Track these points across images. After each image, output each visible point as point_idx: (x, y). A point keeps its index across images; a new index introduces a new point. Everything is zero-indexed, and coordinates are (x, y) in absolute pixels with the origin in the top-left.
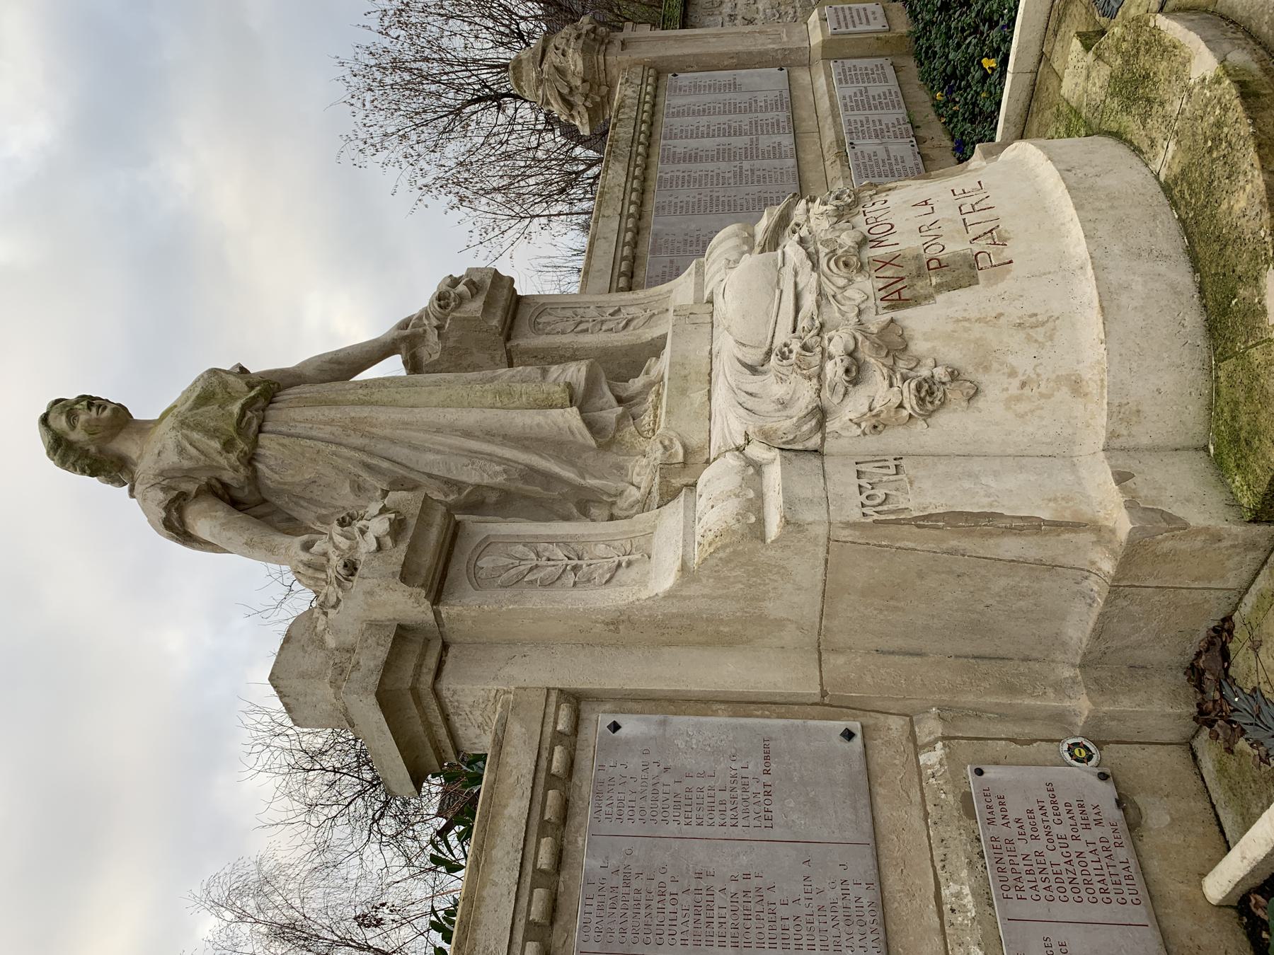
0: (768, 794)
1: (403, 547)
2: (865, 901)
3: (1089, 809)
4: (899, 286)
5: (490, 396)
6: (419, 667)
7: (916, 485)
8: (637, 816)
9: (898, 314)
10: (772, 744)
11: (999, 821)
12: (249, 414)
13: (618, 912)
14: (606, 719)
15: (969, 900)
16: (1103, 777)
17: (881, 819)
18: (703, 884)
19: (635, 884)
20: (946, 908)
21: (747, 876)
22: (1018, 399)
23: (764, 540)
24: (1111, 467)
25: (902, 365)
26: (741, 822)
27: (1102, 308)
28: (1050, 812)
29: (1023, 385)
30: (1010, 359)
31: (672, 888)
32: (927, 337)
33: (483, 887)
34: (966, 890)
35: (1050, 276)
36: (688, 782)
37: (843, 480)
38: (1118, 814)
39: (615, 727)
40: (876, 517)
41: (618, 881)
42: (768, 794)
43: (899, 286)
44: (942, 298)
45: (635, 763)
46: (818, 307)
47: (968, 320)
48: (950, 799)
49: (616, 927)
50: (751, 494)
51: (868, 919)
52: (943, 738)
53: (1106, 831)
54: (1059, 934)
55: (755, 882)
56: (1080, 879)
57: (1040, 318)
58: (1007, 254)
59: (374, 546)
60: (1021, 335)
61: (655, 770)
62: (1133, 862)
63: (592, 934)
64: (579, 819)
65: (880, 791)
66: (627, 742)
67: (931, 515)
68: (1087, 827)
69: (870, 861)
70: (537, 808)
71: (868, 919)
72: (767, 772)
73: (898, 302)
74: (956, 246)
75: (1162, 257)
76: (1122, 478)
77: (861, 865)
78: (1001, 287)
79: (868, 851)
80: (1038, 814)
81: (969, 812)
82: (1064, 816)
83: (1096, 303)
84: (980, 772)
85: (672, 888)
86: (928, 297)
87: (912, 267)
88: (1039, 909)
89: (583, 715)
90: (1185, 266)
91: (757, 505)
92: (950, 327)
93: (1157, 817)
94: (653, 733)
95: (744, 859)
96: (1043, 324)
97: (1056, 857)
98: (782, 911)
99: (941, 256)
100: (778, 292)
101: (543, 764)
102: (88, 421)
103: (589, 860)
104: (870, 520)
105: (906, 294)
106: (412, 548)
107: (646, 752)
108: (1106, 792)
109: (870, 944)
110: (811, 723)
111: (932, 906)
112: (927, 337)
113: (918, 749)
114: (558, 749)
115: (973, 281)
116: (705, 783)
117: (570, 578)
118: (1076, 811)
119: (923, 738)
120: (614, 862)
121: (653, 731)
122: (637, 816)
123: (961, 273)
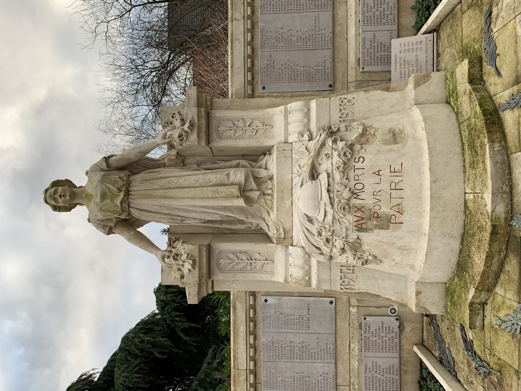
0: (308, 320)
1: (197, 270)
2: (332, 348)
3: (391, 328)
4: (362, 222)
5: (210, 193)
6: (207, 287)
7: (358, 279)
8: (274, 327)
9: (361, 234)
10: (310, 305)
11: (368, 332)
12: (124, 205)
13: (271, 352)
14: (264, 298)
15: (357, 350)
16: (397, 319)
17: (338, 326)
18: (292, 344)
19: (275, 345)
20: (351, 349)
21: (303, 343)
22: (394, 266)
23: (310, 286)
24: (416, 289)
25: (358, 254)
26: (301, 328)
27: (426, 255)
28: (381, 329)
29: (396, 264)
30: (394, 257)
31: (284, 346)
32: (368, 245)
33: (238, 349)
34: (356, 348)
35: (414, 233)
36: (287, 317)
37: (336, 274)
38: (398, 330)
39: (266, 301)
40: (345, 290)
41: (271, 344)
42: (308, 320)
43: (362, 222)
44: (376, 231)
45: (272, 311)
46: (333, 223)
47: (383, 242)
48: (357, 324)
49: (271, 355)
50: (307, 267)
51: (332, 352)
52: (357, 306)
53: (394, 335)
54: (376, 360)
55: (305, 344)
56: (384, 346)
57: (407, 248)
58: (402, 219)
59: (188, 272)
60: (399, 251)
61: (278, 314)
62: (398, 343)
63: (266, 357)
64: (259, 327)
65: (338, 317)
66: (270, 305)
67: (361, 292)
68: (389, 333)
69: (334, 338)
70: (248, 328)
71: (332, 352)
72: (308, 314)
73: (360, 229)
74: (385, 210)
75: (453, 237)
76: (418, 293)
77: (332, 339)
78: (397, 233)
79: (333, 336)
80: (378, 330)
81: (361, 329)
82: (384, 330)
83: (425, 251)
84: (365, 319)
85: (284, 346)
86: (371, 230)
87: (367, 214)
88: (372, 354)
89: (257, 295)
90: (459, 242)
91: (308, 273)
92: (376, 243)
93: (408, 328)
94: (277, 302)
95: (302, 338)
96: (407, 250)
97: (380, 341)
98: (311, 351)
99: (379, 212)
100: (318, 210)
101: (248, 315)
102: (63, 201)
103: (263, 339)
104: (342, 291)
105: (364, 226)
106: (200, 269)
107: (275, 308)
108: (397, 323)
109: (331, 358)
110: (321, 299)
111: (348, 347)
112: (368, 245)
113: (350, 305)
114: (251, 310)
115: (388, 228)
116: (292, 317)
117: (249, 267)
118: (388, 329)
119: (352, 303)
120: (269, 339)
121: (277, 302)
122: (274, 327)
123: (385, 222)
